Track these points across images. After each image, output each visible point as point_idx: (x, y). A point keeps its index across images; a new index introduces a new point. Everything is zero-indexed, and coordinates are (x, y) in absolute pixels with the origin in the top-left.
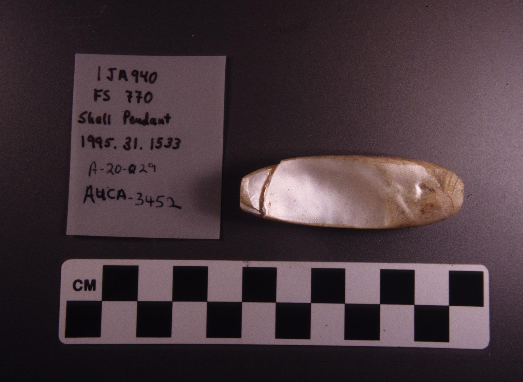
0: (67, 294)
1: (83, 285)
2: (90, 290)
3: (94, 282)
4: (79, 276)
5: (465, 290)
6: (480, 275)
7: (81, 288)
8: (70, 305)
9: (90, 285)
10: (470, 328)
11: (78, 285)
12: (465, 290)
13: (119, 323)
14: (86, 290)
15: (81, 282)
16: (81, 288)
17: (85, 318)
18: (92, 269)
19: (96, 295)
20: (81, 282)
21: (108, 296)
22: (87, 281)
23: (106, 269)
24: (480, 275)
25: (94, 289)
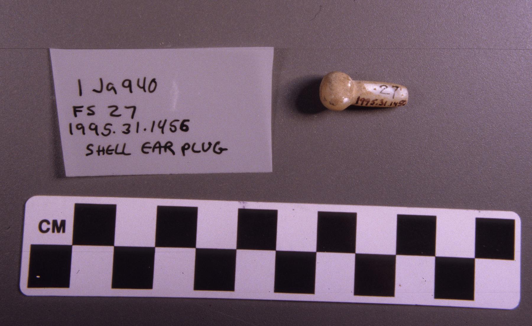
0: (32, 237)
1: (50, 226)
2: (59, 231)
3: (63, 222)
5: (494, 240)
6: (511, 224)
7: (48, 230)
8: (36, 250)
9: (59, 226)
11: (45, 226)
12: (494, 240)
13: (91, 272)
14: (53, 231)
15: (48, 223)
16: (48, 230)
17: (52, 265)
19: (65, 238)
20: (48, 223)
21: (81, 238)
22: (55, 222)
23: (80, 209)
24: (511, 224)
25: (64, 231)
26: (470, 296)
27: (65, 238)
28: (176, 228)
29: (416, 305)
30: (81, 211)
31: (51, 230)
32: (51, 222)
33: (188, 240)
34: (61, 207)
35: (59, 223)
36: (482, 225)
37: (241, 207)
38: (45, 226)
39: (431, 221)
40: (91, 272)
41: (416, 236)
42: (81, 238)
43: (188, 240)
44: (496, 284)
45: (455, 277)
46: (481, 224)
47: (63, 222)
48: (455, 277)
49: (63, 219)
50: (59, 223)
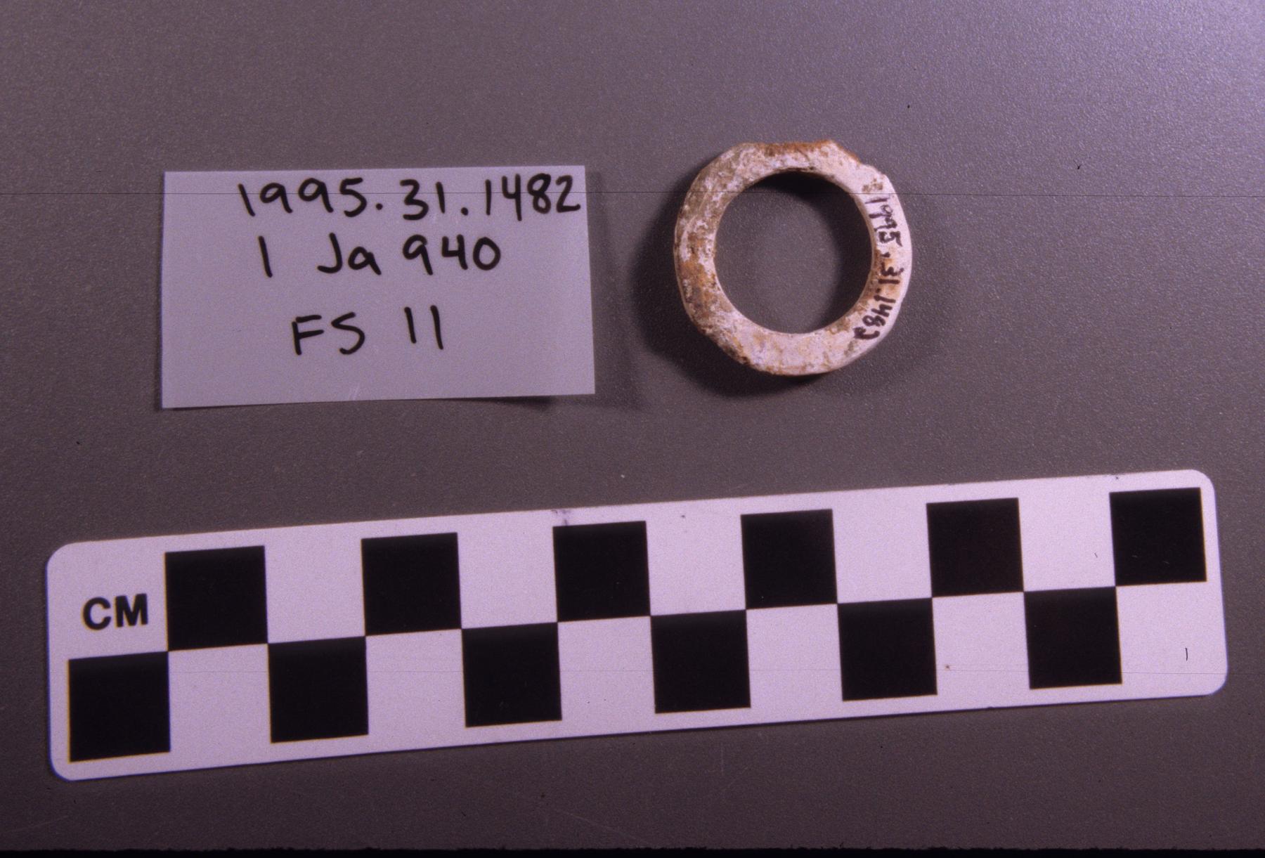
0: (69, 641)
1: (112, 612)
2: (132, 622)
3: (141, 600)
4: (99, 587)
5: (1155, 540)
6: (1192, 496)
7: (107, 621)
8: (81, 671)
10: (1173, 641)
11: (98, 614)
12: (1155, 540)
13: (220, 710)
14: (120, 624)
15: (106, 604)
16: (107, 621)
17: (124, 703)
18: (134, 564)
19: (150, 636)
20: (106, 604)
22: (121, 601)
23: (177, 565)
24: (1192, 496)
25: (145, 621)
26: (1112, 674)
27: (150, 636)
28: (411, 586)
29: (990, 709)
30: (180, 569)
31: (113, 622)
32: (112, 602)
33: (441, 610)
34: (134, 564)
35: (131, 603)
36: (1125, 508)
37: (559, 523)
38: (98, 614)
39: (1007, 512)
40: (220, 710)
41: (975, 549)
42: (186, 633)
43: (441, 610)
44: (1173, 641)
45: (1073, 636)
46: (1122, 505)
47: (141, 600)
48: (1073, 636)
49: (140, 592)
50: (131, 603)
